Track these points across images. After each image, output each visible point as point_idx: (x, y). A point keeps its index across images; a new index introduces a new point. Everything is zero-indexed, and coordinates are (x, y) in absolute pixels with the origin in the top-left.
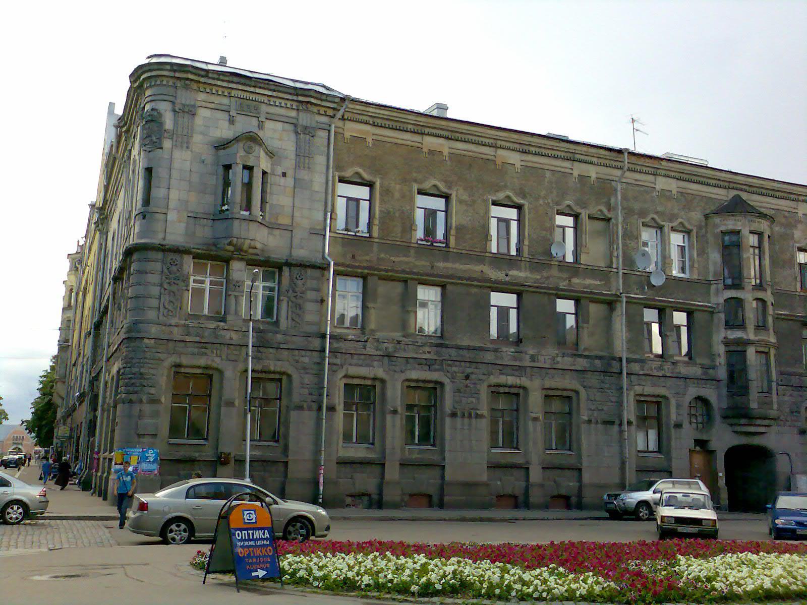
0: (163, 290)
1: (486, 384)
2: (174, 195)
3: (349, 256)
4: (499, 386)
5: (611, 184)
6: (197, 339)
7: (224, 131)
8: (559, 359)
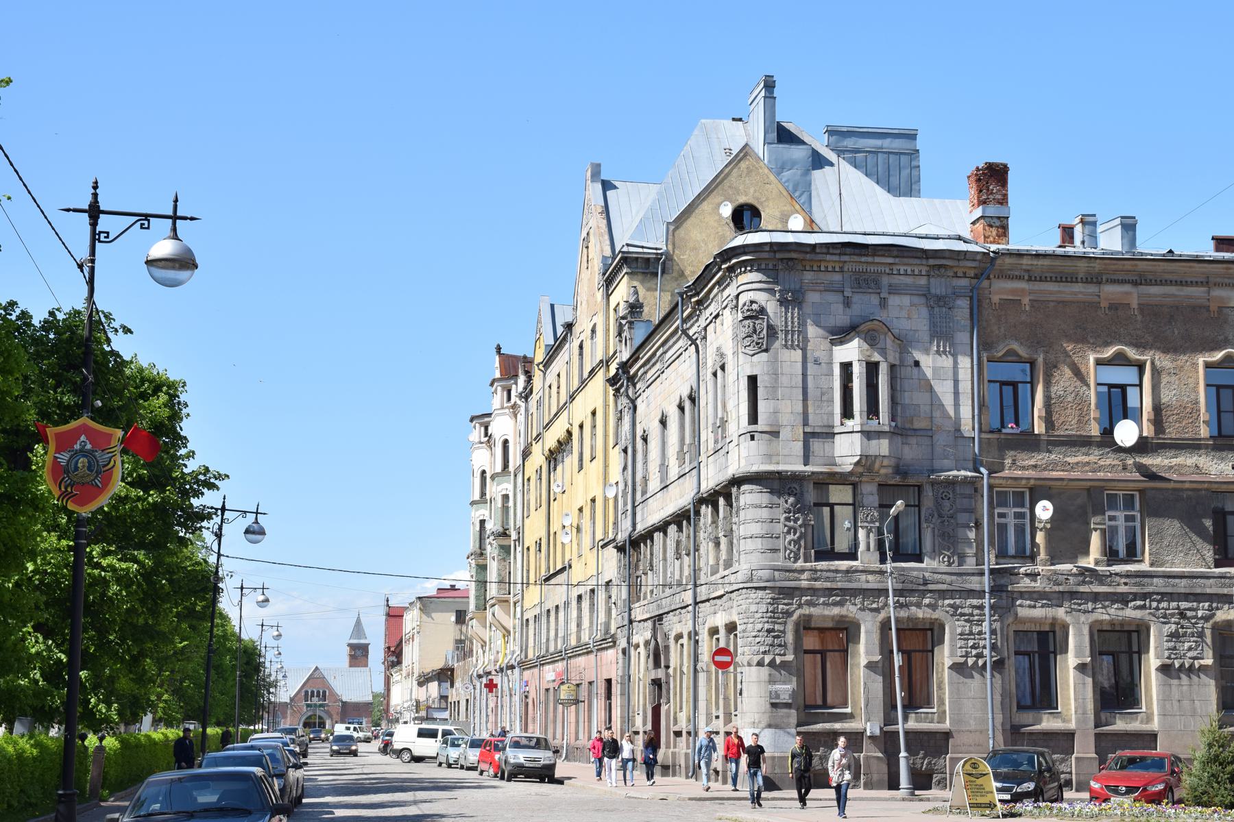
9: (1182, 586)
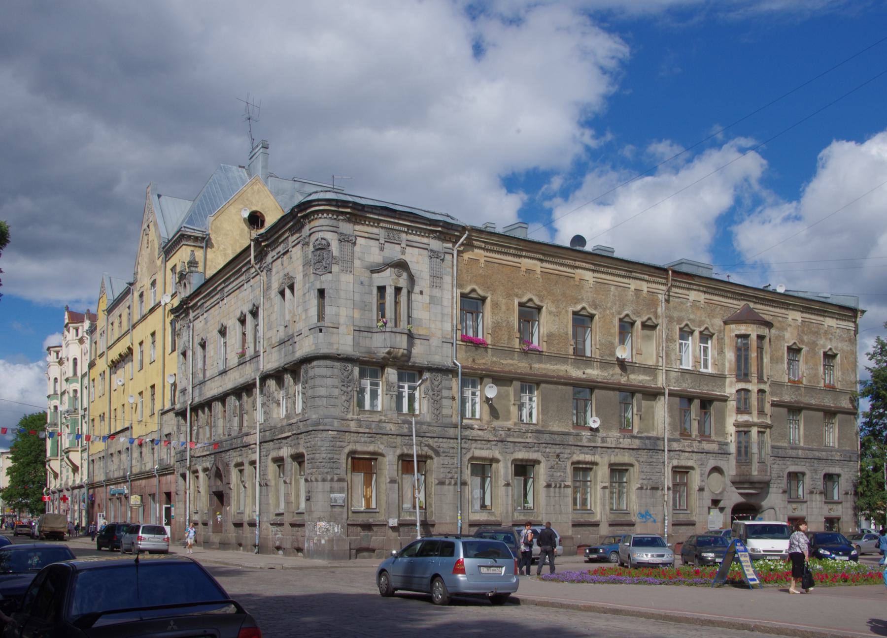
1: (570, 462)
2: (343, 312)
3: (470, 360)
4: (579, 462)
5: (657, 296)
6: (367, 431)
8: (621, 440)
9: (558, 439)
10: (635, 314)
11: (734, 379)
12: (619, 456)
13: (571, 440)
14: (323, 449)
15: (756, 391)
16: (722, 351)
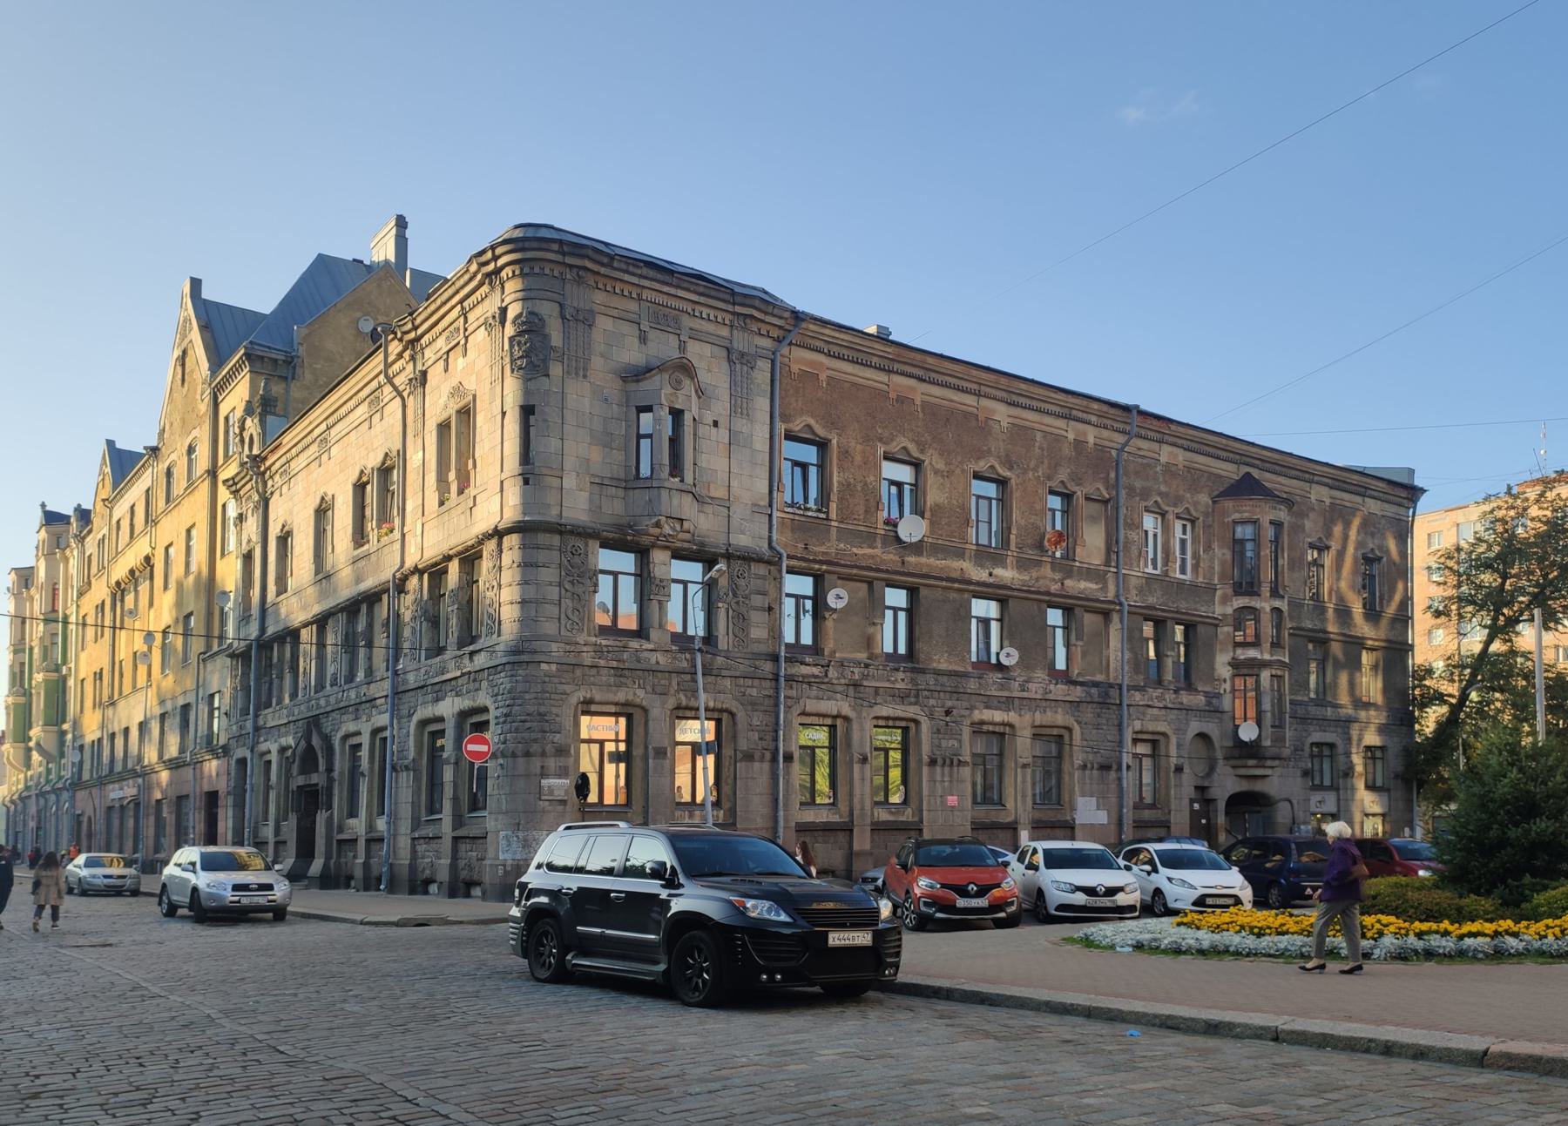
0: (563, 592)
3: (801, 545)
4: (982, 723)
7: (633, 355)
10: (1073, 480)
11: (1230, 591)
12: (1049, 713)
13: (972, 685)
14: (527, 696)
15: (1268, 609)
16: (1210, 547)
